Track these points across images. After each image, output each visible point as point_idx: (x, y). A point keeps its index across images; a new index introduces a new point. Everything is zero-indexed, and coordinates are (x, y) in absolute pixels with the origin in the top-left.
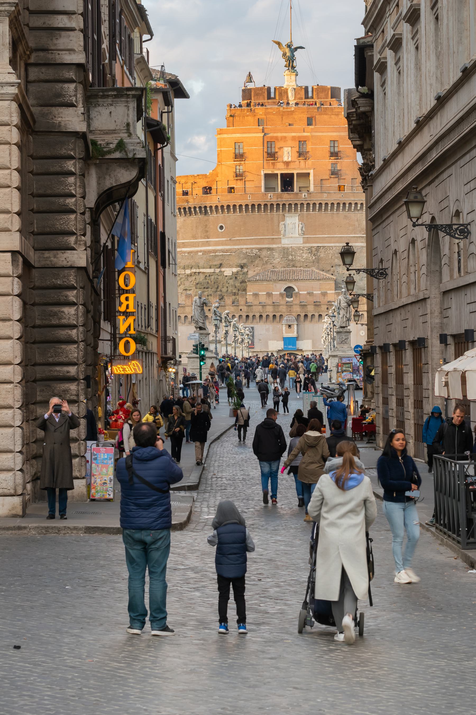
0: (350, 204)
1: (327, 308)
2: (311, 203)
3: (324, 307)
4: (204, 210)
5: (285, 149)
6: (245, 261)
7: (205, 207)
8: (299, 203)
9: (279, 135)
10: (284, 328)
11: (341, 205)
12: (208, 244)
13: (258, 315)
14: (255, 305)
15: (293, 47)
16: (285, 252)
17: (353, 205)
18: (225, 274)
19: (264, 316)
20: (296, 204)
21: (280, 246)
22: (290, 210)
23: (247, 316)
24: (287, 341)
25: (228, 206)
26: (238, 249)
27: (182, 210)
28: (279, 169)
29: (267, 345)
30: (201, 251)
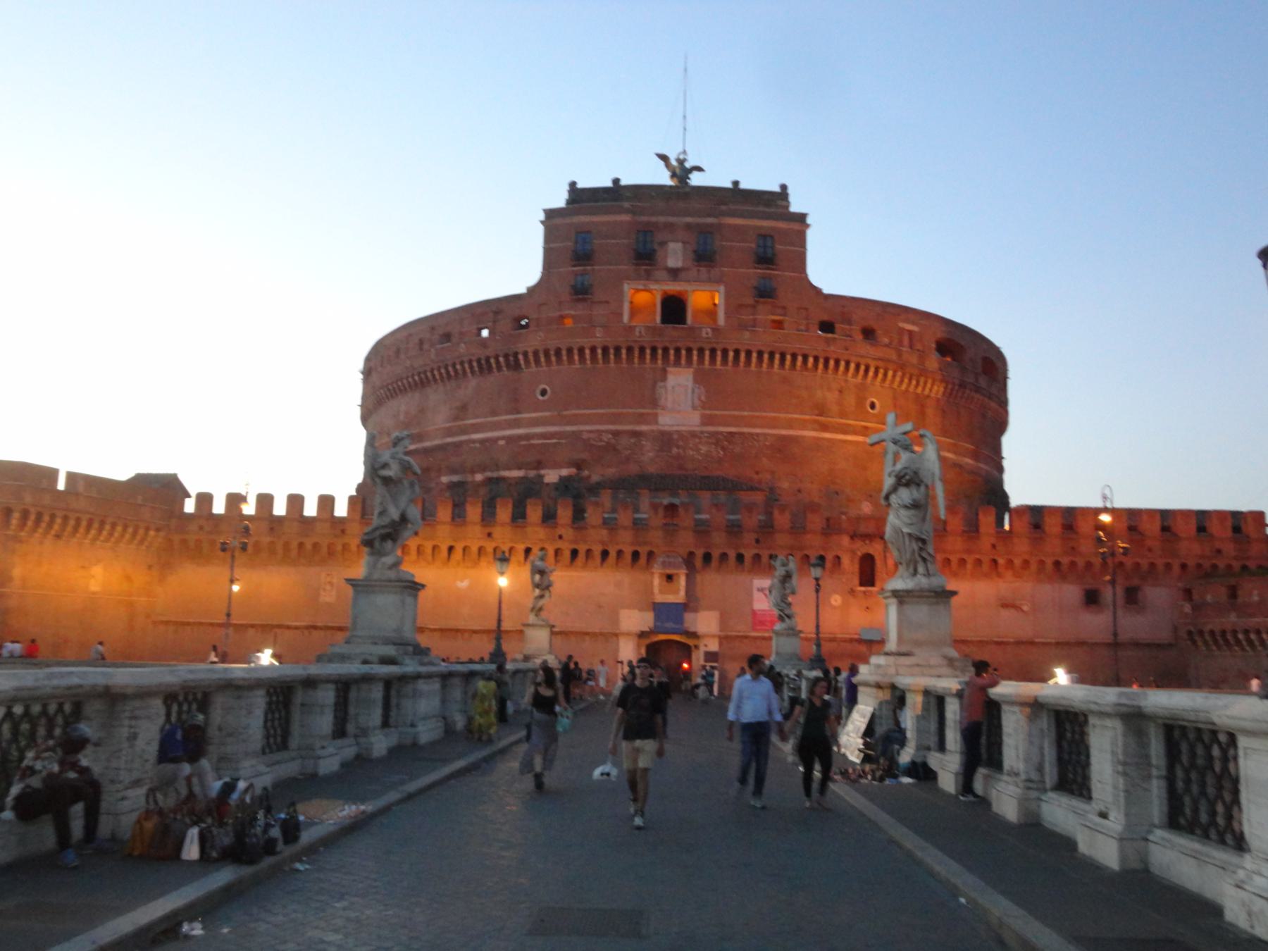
0: (794, 356)
1: (757, 541)
2: (719, 347)
3: (749, 538)
4: (513, 363)
5: (672, 246)
6: (584, 456)
7: (516, 355)
8: (695, 346)
9: (662, 219)
10: (656, 581)
11: (777, 356)
12: (516, 424)
13: (597, 550)
14: (594, 527)
15: (688, 165)
16: (666, 440)
17: (800, 358)
18: (547, 480)
19: (613, 554)
20: (689, 350)
21: (654, 428)
22: (677, 362)
23: (574, 553)
24: (660, 610)
25: (558, 352)
26: (573, 432)
27: (475, 364)
28: (657, 281)
29: (615, 620)
30: (503, 438)
